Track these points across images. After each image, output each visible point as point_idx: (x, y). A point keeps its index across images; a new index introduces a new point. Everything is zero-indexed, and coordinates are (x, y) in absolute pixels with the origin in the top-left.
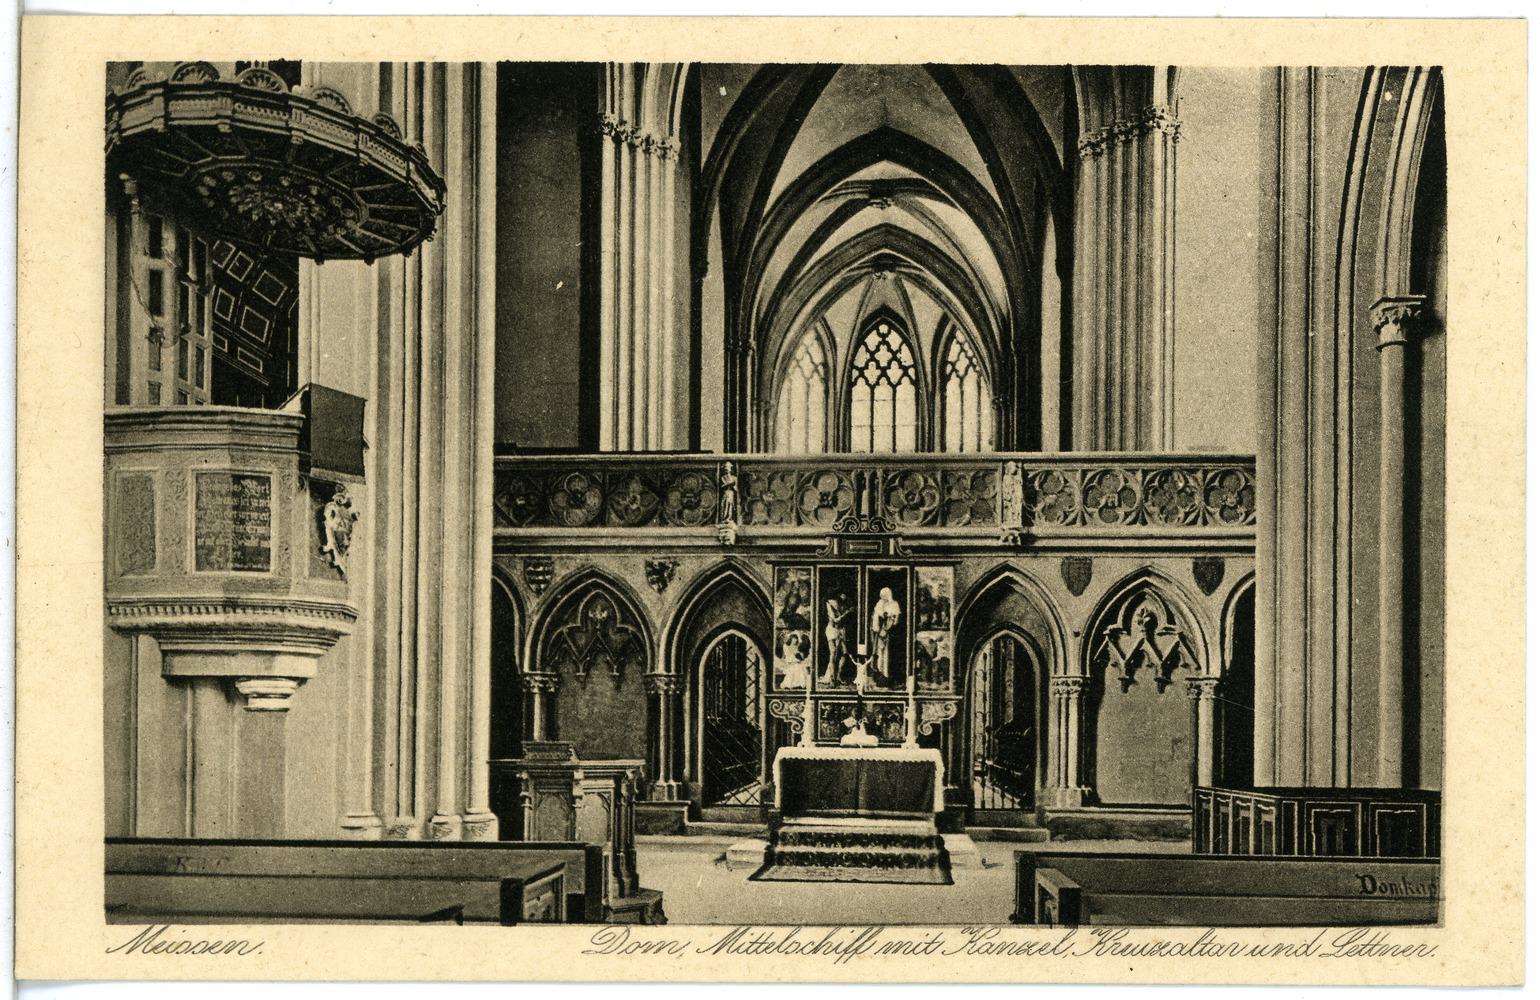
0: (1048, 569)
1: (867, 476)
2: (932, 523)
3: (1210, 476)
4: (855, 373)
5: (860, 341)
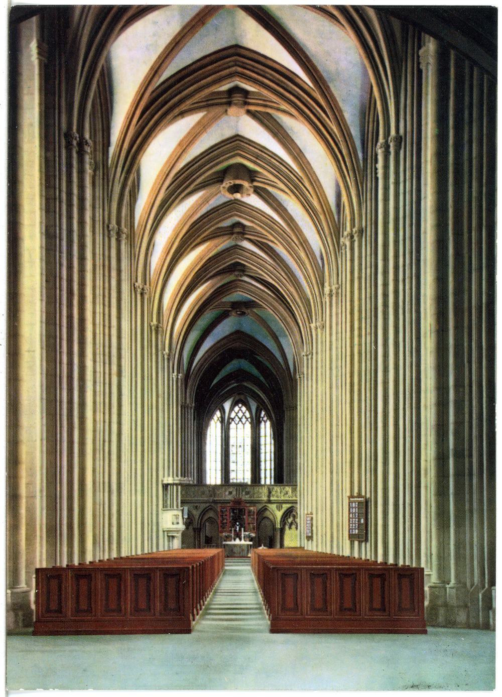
0: (273, 507)
4: (231, 420)
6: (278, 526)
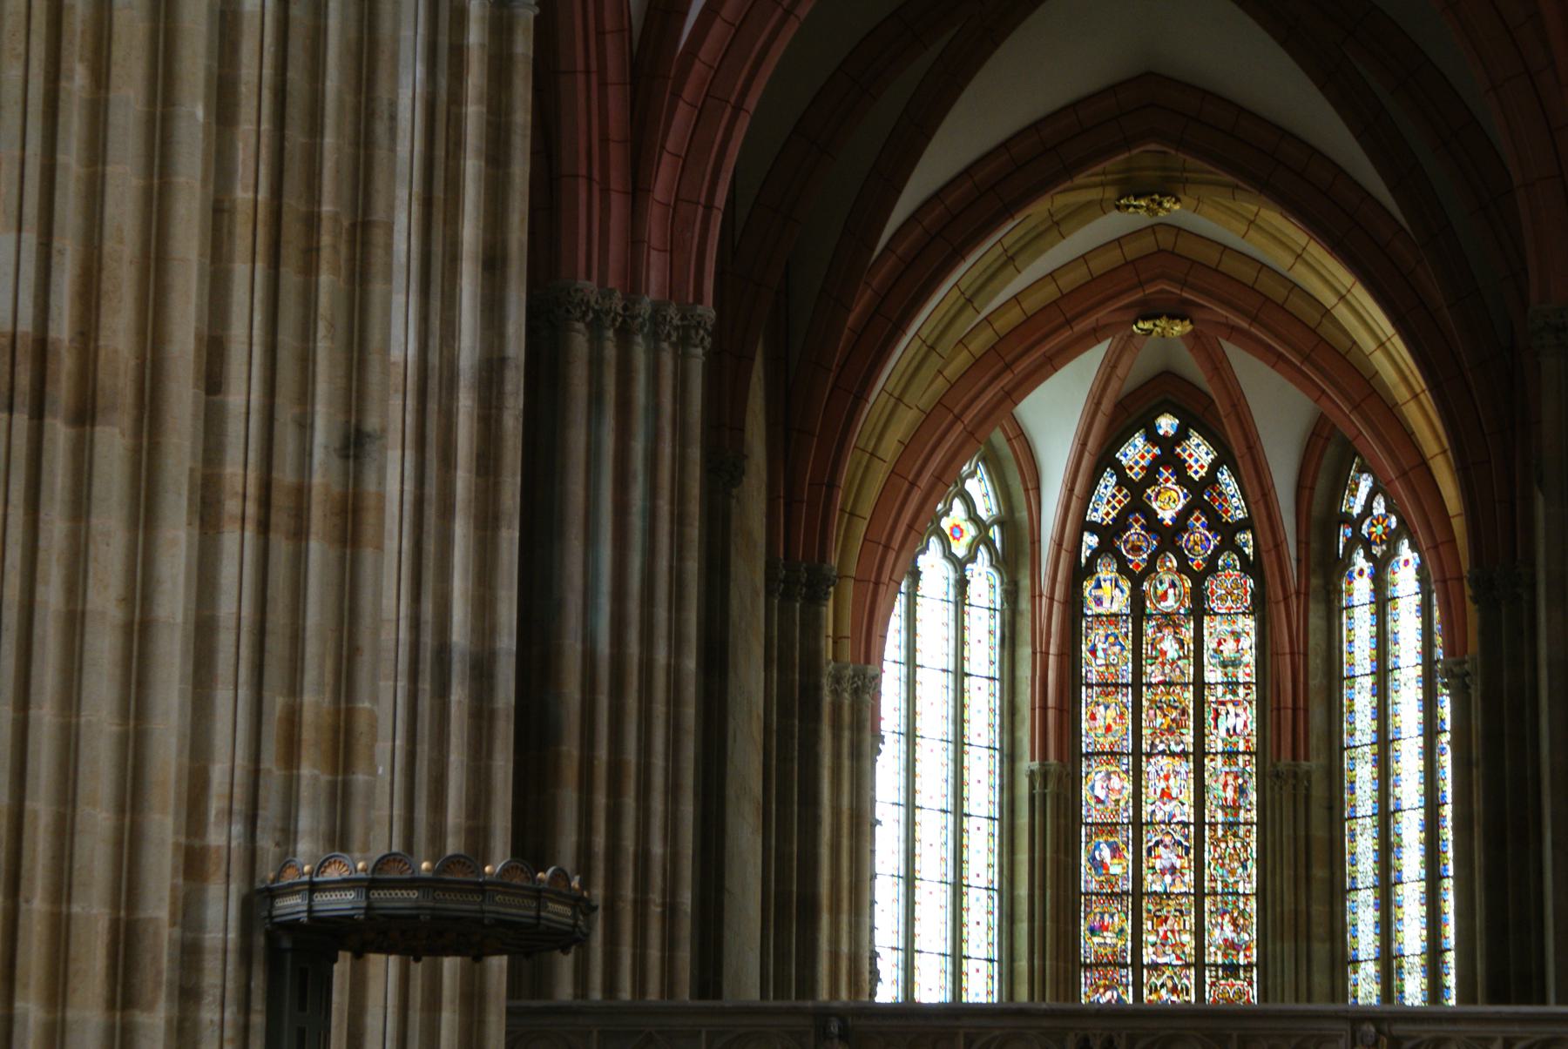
5: (1105, 459)
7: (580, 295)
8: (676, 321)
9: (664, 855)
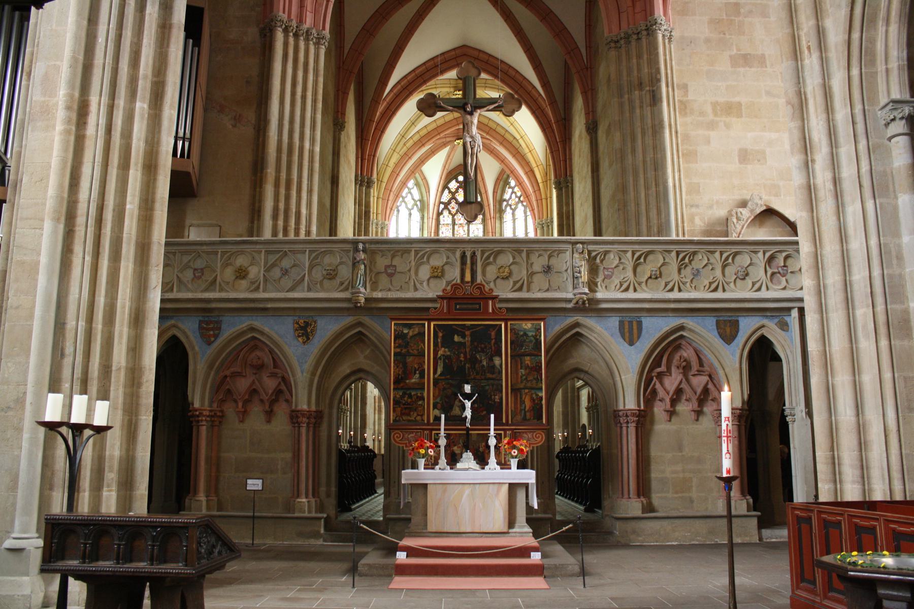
1: (468, 255)
2: (520, 289)
3: (725, 255)
6: (629, 401)
7: (280, 18)
8: (315, 35)
9: (307, 214)
